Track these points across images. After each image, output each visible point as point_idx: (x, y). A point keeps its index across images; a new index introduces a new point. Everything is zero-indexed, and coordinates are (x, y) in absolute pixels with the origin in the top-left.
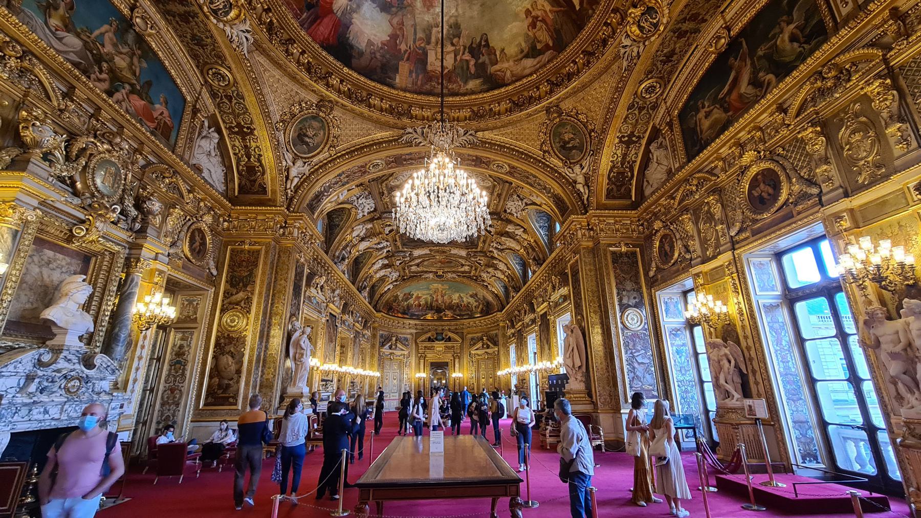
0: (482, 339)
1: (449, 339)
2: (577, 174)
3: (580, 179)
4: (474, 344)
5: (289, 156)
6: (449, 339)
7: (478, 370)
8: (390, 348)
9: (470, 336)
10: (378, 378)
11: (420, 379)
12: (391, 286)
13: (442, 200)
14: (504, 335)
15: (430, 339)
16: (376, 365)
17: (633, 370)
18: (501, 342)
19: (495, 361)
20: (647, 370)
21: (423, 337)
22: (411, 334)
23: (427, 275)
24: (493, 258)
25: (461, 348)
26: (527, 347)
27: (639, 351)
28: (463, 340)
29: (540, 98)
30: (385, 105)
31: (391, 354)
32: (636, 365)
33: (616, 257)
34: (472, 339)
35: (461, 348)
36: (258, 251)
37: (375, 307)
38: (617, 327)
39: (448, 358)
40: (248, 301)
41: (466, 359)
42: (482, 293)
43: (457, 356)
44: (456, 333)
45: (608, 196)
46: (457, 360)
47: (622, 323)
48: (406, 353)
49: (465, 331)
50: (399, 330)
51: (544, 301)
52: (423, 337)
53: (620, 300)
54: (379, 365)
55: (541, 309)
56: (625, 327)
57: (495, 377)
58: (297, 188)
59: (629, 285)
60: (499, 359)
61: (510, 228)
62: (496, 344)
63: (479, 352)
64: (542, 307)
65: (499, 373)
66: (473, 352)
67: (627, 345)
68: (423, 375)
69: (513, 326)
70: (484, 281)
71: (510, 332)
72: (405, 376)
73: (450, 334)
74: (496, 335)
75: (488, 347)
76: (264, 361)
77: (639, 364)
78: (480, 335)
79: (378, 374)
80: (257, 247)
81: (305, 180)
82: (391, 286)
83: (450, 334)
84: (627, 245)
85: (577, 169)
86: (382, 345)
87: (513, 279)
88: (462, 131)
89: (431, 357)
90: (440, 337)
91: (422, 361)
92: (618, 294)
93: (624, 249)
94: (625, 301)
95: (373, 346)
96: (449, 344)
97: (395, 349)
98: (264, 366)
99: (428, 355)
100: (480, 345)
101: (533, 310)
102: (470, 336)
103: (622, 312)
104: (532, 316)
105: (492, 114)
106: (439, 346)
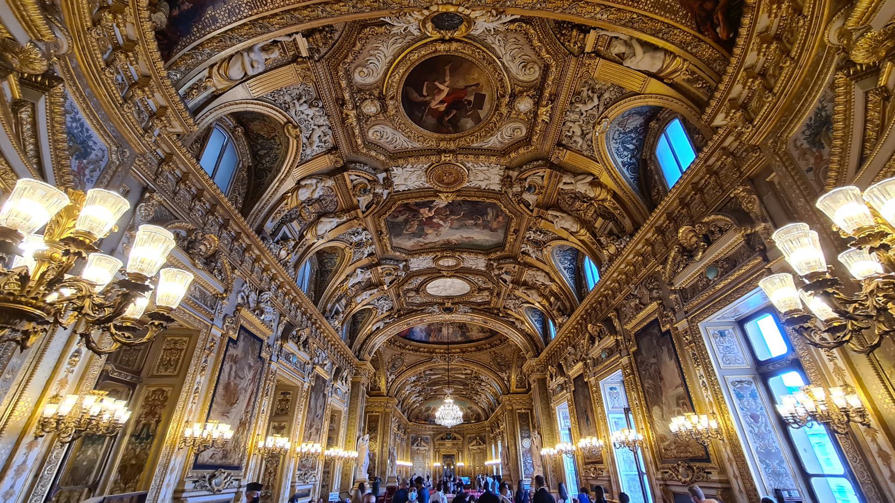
1: (455, 438)
6: (455, 438)
7: (474, 459)
13: (449, 413)
17: (525, 466)
19: (484, 455)
21: (438, 437)
25: (463, 444)
28: (463, 437)
33: (520, 415)
35: (463, 444)
39: (454, 452)
40: (376, 437)
41: (466, 452)
42: (475, 407)
43: (460, 450)
52: (438, 437)
57: (484, 466)
59: (525, 428)
62: (484, 442)
65: (486, 463)
71: (492, 435)
73: (455, 435)
83: (455, 435)
89: (443, 451)
96: (455, 442)
100: (474, 442)
101: (499, 428)
106: (449, 443)
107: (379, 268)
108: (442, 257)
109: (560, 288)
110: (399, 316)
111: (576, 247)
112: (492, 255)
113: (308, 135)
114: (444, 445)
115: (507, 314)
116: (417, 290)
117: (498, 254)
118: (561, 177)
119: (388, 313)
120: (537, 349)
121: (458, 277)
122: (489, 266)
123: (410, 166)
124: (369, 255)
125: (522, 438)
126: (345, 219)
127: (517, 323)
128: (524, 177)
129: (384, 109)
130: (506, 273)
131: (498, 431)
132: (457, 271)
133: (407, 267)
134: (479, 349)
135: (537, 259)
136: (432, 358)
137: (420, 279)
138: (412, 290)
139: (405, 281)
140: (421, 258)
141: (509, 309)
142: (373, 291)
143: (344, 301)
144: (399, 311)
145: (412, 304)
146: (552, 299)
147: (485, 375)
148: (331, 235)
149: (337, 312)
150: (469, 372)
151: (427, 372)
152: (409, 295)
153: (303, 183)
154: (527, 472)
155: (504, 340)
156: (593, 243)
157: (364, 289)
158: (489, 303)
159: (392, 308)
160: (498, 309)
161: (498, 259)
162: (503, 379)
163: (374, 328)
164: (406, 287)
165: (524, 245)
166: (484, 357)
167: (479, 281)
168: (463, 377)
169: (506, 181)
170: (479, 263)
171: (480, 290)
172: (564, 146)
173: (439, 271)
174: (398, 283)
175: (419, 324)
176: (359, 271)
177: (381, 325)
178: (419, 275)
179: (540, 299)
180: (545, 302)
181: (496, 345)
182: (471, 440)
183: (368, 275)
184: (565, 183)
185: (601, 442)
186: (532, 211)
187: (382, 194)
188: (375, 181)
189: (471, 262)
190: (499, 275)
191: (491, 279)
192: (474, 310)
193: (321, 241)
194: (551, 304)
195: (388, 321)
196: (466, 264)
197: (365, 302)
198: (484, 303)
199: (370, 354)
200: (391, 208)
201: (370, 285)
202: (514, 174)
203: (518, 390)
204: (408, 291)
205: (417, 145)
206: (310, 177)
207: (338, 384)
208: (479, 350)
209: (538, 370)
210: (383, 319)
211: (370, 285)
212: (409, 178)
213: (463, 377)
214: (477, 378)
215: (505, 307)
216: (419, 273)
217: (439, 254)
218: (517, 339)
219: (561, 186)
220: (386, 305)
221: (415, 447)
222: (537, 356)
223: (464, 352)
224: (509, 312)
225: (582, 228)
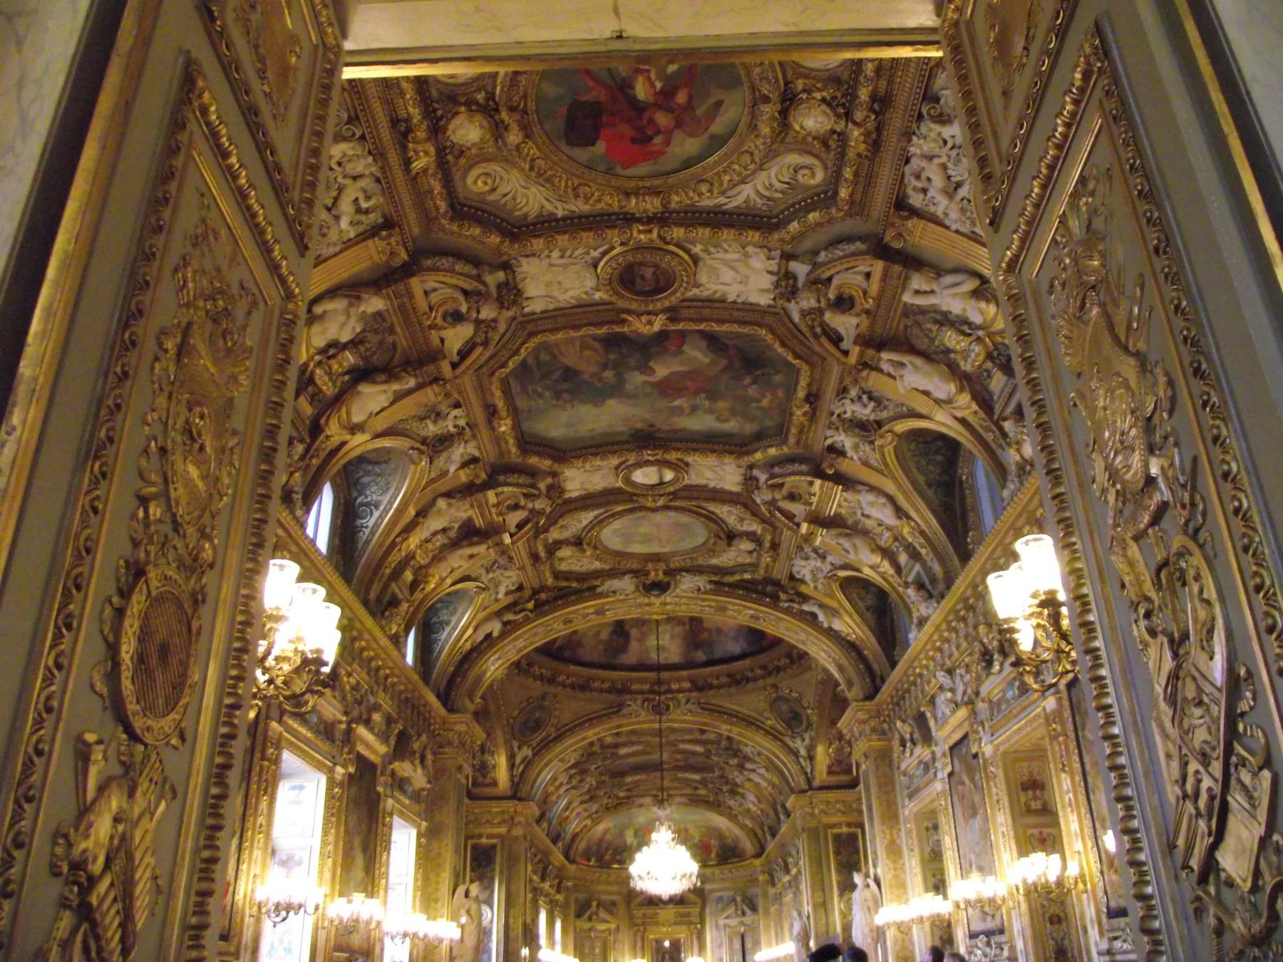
0: (734, 900)
2: (800, 746)
3: (803, 752)
4: (723, 910)
5: (515, 744)
8: (590, 919)
14: (765, 895)
16: (571, 947)
22: (620, 894)
23: (642, 800)
24: (736, 785)
29: (755, 680)
30: (606, 685)
31: (590, 930)
33: (837, 838)
34: (720, 899)
36: (494, 847)
37: (567, 856)
45: (830, 772)
48: (613, 926)
50: (601, 888)
54: (575, 949)
58: (523, 772)
61: (749, 766)
62: (754, 909)
69: (773, 885)
70: (730, 808)
71: (772, 891)
75: (744, 914)
78: (731, 893)
80: (494, 841)
81: (528, 763)
84: (849, 825)
85: (798, 742)
86: (579, 915)
88: (683, 701)
91: (639, 939)
93: (845, 830)
96: (682, 910)
100: (732, 910)
101: (787, 871)
105: (711, 687)
107: (491, 496)
108: (640, 465)
109: (922, 533)
110: (536, 606)
111: (951, 434)
112: (758, 456)
113: (329, 202)
115: (800, 595)
116: (578, 542)
117: (772, 451)
118: (907, 278)
119: (511, 599)
120: (873, 680)
121: (676, 509)
122: (750, 481)
123: (556, 254)
124: (464, 465)
126: (412, 383)
127: (821, 617)
128: (825, 276)
129: (498, 130)
130: (792, 497)
131: (786, 879)
132: (675, 495)
133: (555, 490)
134: (737, 681)
135: (866, 464)
136: (620, 706)
137: (587, 517)
138: (566, 542)
139: (553, 520)
140: (588, 466)
141: (802, 581)
142: (474, 550)
143: (409, 576)
144: (535, 592)
145: (568, 576)
146: (903, 558)
147: (753, 742)
148: (380, 424)
149: (394, 602)
150: (712, 736)
151: (609, 740)
152: (560, 554)
153: (318, 310)
155: (798, 658)
156: (987, 429)
157: (455, 544)
158: (754, 567)
159: (520, 588)
160: (777, 583)
161: (771, 465)
162: (796, 754)
163: (480, 637)
164: (554, 534)
165: (829, 433)
166: (753, 701)
167: (730, 515)
168: (699, 749)
169: (787, 286)
170: (723, 473)
171: (731, 537)
172: (915, 213)
173: (630, 497)
174: (534, 525)
175: (582, 618)
176: (442, 503)
177: (495, 627)
178: (586, 508)
179: (876, 559)
180: (886, 566)
181: (778, 669)
183: (462, 511)
184: (917, 292)
186: (846, 353)
187: (495, 321)
188: (479, 293)
189: (710, 475)
190: (773, 503)
191: (755, 514)
192: (720, 587)
193: (360, 438)
194: (898, 569)
195: (509, 617)
196: (693, 478)
197: (457, 575)
198: (742, 568)
199: (471, 696)
200: (517, 352)
201: (469, 534)
202: (800, 269)
203: (834, 779)
204: (559, 544)
205: (580, 207)
206: (332, 293)
207: (404, 768)
208: (738, 683)
209: (873, 730)
210: (498, 614)
211: (469, 534)
212: (557, 279)
213: (699, 749)
214: (736, 753)
215: (792, 577)
216: (587, 501)
217: (632, 458)
218: (823, 654)
219: (907, 298)
220: (508, 579)
222: (870, 697)
223: (700, 689)
224: (803, 589)
225: (961, 390)
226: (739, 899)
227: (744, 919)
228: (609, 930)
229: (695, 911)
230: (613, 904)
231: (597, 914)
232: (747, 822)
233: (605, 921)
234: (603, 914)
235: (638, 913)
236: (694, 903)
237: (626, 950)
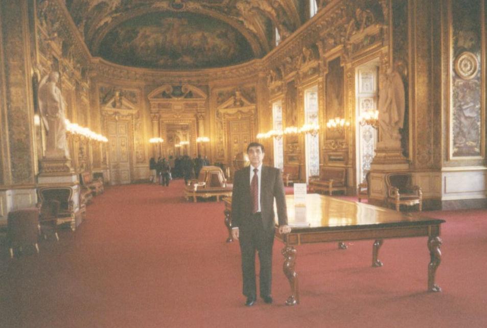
0: (234, 95)
1: (190, 95)
4: (223, 101)
8: (114, 105)
9: (217, 91)
10: (104, 144)
11: (154, 146)
12: (109, 19)
15: (164, 95)
16: (99, 127)
18: (260, 97)
20: (473, 125)
26: (302, 103)
27: (467, 104)
28: (208, 94)
31: (116, 113)
32: (463, 119)
34: (220, 94)
38: (447, 75)
44: (199, 87)
46: (201, 122)
47: (454, 70)
48: (134, 112)
49: (211, 84)
51: (336, 44)
53: (456, 42)
55: (335, 51)
56: (457, 76)
60: (256, 119)
62: (252, 100)
63: (230, 111)
64: (333, 51)
66: (222, 111)
67: (456, 96)
68: (157, 140)
72: (135, 142)
74: (253, 90)
75: (242, 105)
76: (10, 116)
77: (466, 118)
78: (230, 89)
79: (104, 139)
82: (109, 19)
83: (191, 88)
86: (104, 102)
87: (285, 13)
90: (178, 92)
91: (156, 122)
92: (455, 34)
94: (461, 43)
95: (93, 103)
96: (191, 101)
97: (119, 108)
98: (10, 124)
99: (164, 115)
102: (217, 91)
103: (457, 56)
104: (314, 64)
114: (167, 106)
125: (458, 53)
154: (462, 142)
182: (222, 99)
185: (348, 124)
221: (108, 108)
226: (237, 93)
227: (241, 109)
228: (132, 115)
229: (200, 103)
230: (133, 95)
231: (120, 101)
232: (252, 28)
233: (131, 109)
234: (125, 102)
235: (154, 102)
236: (201, 97)
237: (145, 128)
